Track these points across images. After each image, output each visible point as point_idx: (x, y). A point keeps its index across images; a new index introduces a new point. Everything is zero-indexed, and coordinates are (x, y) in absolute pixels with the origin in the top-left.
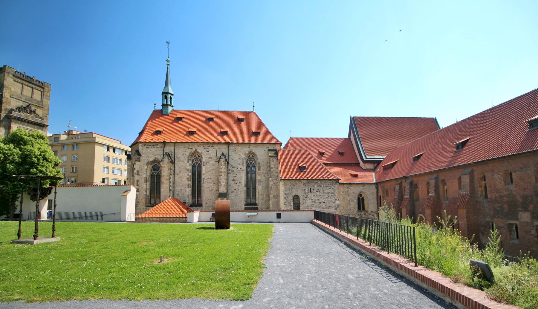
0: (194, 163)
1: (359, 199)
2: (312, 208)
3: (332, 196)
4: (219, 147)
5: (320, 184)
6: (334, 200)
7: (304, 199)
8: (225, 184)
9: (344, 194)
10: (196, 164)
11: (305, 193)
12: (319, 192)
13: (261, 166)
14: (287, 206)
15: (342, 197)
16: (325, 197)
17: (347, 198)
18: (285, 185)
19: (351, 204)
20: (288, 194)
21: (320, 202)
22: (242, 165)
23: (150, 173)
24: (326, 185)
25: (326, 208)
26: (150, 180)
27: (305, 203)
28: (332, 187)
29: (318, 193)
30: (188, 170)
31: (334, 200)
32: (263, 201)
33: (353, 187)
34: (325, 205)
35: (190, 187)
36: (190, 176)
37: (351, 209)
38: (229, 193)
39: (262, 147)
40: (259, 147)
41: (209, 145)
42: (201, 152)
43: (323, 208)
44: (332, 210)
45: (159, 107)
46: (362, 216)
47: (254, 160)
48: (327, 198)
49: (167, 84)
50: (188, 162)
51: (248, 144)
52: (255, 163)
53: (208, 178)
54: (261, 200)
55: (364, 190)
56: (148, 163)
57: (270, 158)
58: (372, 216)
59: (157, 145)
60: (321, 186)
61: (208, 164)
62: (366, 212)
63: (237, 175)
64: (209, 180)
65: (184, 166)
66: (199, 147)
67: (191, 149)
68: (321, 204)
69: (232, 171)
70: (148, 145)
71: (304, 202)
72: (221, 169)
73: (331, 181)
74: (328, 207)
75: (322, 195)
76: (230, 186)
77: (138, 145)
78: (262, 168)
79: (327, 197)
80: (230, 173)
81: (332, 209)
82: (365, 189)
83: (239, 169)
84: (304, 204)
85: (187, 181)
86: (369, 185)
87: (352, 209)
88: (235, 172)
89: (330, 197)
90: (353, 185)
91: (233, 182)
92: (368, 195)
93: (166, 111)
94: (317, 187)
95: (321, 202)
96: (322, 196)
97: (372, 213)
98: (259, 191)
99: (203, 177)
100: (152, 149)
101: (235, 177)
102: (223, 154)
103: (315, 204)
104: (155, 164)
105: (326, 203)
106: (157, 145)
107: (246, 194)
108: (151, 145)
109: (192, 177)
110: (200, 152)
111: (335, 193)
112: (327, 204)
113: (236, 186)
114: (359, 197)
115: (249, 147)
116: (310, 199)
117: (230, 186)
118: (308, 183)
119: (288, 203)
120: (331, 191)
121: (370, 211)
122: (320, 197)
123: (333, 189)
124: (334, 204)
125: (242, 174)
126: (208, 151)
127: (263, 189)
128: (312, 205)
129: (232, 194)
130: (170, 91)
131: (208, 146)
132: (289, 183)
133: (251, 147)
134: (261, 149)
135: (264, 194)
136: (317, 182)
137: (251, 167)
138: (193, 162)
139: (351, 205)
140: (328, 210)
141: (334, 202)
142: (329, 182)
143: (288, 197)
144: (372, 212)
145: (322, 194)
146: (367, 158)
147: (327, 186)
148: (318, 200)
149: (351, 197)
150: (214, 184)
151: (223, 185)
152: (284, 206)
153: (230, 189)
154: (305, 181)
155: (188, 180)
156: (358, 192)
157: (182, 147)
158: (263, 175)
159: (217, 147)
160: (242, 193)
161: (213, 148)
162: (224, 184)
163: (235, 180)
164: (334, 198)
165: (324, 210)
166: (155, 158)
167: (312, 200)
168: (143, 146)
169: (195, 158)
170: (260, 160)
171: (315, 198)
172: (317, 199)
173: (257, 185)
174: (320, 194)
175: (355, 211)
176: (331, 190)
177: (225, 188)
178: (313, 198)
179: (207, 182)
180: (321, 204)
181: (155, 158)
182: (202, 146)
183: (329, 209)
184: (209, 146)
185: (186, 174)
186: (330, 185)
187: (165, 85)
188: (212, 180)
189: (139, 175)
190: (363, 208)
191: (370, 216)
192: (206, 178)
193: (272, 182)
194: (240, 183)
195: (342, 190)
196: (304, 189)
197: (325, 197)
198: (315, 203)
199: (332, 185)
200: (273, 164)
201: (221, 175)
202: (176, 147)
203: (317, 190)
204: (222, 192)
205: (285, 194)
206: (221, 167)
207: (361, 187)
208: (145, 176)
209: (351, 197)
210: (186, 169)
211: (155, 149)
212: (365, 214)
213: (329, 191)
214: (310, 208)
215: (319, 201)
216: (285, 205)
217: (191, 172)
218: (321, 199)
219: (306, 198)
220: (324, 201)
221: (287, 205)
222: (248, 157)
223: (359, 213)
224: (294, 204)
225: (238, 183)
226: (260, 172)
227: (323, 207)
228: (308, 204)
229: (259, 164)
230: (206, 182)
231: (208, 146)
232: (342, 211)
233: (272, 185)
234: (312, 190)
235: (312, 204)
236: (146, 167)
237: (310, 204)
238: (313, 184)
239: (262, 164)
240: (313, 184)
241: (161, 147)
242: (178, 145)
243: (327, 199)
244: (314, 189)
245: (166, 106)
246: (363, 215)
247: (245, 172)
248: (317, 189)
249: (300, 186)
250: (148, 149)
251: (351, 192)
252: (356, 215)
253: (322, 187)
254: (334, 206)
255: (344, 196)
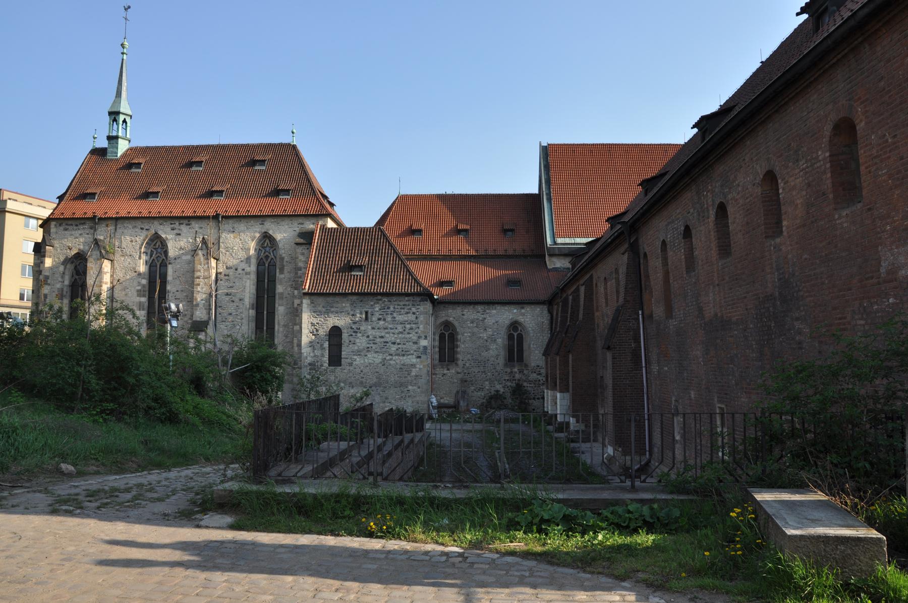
0: (153, 260)
1: (510, 337)
2: (367, 354)
3: (411, 329)
4: (202, 226)
5: (386, 303)
6: (415, 338)
7: (352, 335)
8: (206, 302)
9: (475, 325)
10: (156, 261)
11: (355, 323)
12: (384, 320)
13: (285, 263)
14: (314, 349)
15: (470, 332)
16: (397, 331)
17: (481, 335)
18: (313, 305)
19: (489, 349)
20: (317, 323)
21: (385, 342)
22: (247, 263)
23: (71, 281)
24: (398, 305)
25: (398, 355)
26: (69, 294)
27: (354, 344)
28: (414, 310)
29: (382, 323)
30: (140, 274)
31: (415, 338)
32: (288, 341)
33: (495, 309)
34: (395, 349)
35: (143, 310)
36: (144, 286)
37: (488, 360)
38: (217, 321)
39: (288, 225)
40: (283, 223)
41: (182, 222)
42: (166, 237)
43: (392, 355)
44: (410, 359)
45: (103, 143)
46: (513, 377)
47: (273, 251)
48: (401, 333)
49: (119, 94)
50: (140, 258)
51: (261, 218)
52: (276, 257)
53: (177, 291)
54: (284, 338)
55: (521, 317)
56: (66, 261)
57: (297, 247)
58: (539, 376)
59: (84, 224)
60: (389, 308)
61: (178, 261)
62: (523, 368)
63: (234, 285)
64: (179, 295)
65: (132, 265)
66: (161, 226)
67: (146, 229)
68: (388, 347)
69: (225, 275)
70: (67, 224)
71: (350, 341)
72: (200, 271)
73: (410, 298)
74: (403, 353)
75: (390, 326)
76: (220, 307)
77: (50, 224)
78: (286, 271)
79: (401, 330)
80: (221, 280)
81: (409, 357)
82: (523, 315)
83: (240, 271)
84: (350, 346)
85: (138, 296)
86: (533, 306)
87: (493, 359)
88: (231, 277)
89: (407, 331)
90: (496, 305)
91: (227, 299)
92: (530, 329)
93: (115, 150)
94: (380, 309)
95: (387, 342)
96: (391, 329)
97: (538, 370)
98: (280, 318)
99: (168, 288)
100: (73, 232)
101: (231, 287)
102: (204, 242)
103: (374, 346)
104: (79, 261)
105: (398, 344)
106: (82, 224)
107: (253, 325)
108: (72, 225)
109: (147, 289)
110: (163, 236)
111: (418, 323)
112: (399, 346)
113: (231, 308)
114: (512, 332)
115: (263, 224)
116: (363, 336)
117: (220, 307)
118: (361, 301)
119: (318, 343)
120: (411, 317)
121: (533, 364)
122: (386, 331)
123: (414, 313)
124: (415, 347)
125: (246, 282)
126: (180, 234)
127: (287, 314)
128: (368, 348)
129: (224, 323)
130: (122, 110)
131: (180, 224)
132: (320, 301)
133: (265, 223)
134: (286, 227)
135: (290, 324)
136: (380, 300)
137: (267, 265)
138: (151, 256)
139: (491, 352)
140: (401, 358)
141: (415, 343)
142: (406, 298)
143: (317, 330)
144: (538, 366)
145: (390, 324)
146: (555, 243)
147: (401, 308)
148: (382, 337)
149: (490, 331)
150: (188, 302)
151: (201, 306)
152: (309, 349)
153: (220, 314)
154: (355, 298)
155: (140, 293)
156: (507, 322)
157: (130, 227)
158: (290, 284)
159: (197, 225)
160: (245, 321)
161: (189, 227)
162: (204, 302)
163: (230, 295)
164: (416, 333)
165: (394, 358)
166: (79, 249)
167: (368, 337)
168: (58, 225)
169: (155, 249)
170: (283, 252)
171: (374, 333)
172: (378, 334)
173: (277, 305)
174: (387, 324)
175: (498, 364)
176: (409, 315)
177: (205, 312)
178: (371, 333)
179: (176, 299)
180: (388, 347)
181: (79, 249)
182: (169, 222)
183: (405, 358)
184: (182, 224)
185: (135, 283)
186: (409, 305)
187: (116, 97)
188: (185, 294)
189: (49, 284)
190: (521, 359)
191: (534, 376)
192: (174, 290)
193: (299, 298)
194: (240, 300)
195: (472, 317)
196: (352, 313)
197: (397, 331)
198: (374, 343)
199: (413, 305)
200: (303, 259)
201: (199, 285)
202: (118, 226)
203: (381, 316)
204: (198, 319)
205: (313, 324)
206: (199, 268)
207: (515, 311)
208: (59, 286)
209: (491, 333)
210: (135, 272)
211: (80, 232)
212: (521, 371)
213: (406, 319)
214: (362, 354)
215: (382, 340)
216: (310, 346)
217: (147, 276)
218: (387, 335)
219: (357, 332)
220: (393, 338)
221: (316, 347)
222: (262, 244)
223: (509, 370)
224: (329, 345)
225: (237, 300)
226: (282, 276)
227: (392, 352)
228: (359, 344)
229: (282, 259)
230: (173, 298)
231: (180, 224)
232: (467, 365)
233: (298, 305)
234: (369, 315)
235: (368, 345)
236: (62, 268)
237: (365, 345)
238: (372, 303)
239: (288, 260)
240: (372, 303)
241: (91, 228)
242: (122, 224)
243: (400, 335)
244: (373, 315)
245: (115, 141)
246: (516, 373)
247: (253, 277)
248: (380, 315)
249: (345, 307)
250: (66, 232)
251: (490, 321)
252: (499, 374)
253: (392, 309)
254: (415, 351)
255: (476, 330)
